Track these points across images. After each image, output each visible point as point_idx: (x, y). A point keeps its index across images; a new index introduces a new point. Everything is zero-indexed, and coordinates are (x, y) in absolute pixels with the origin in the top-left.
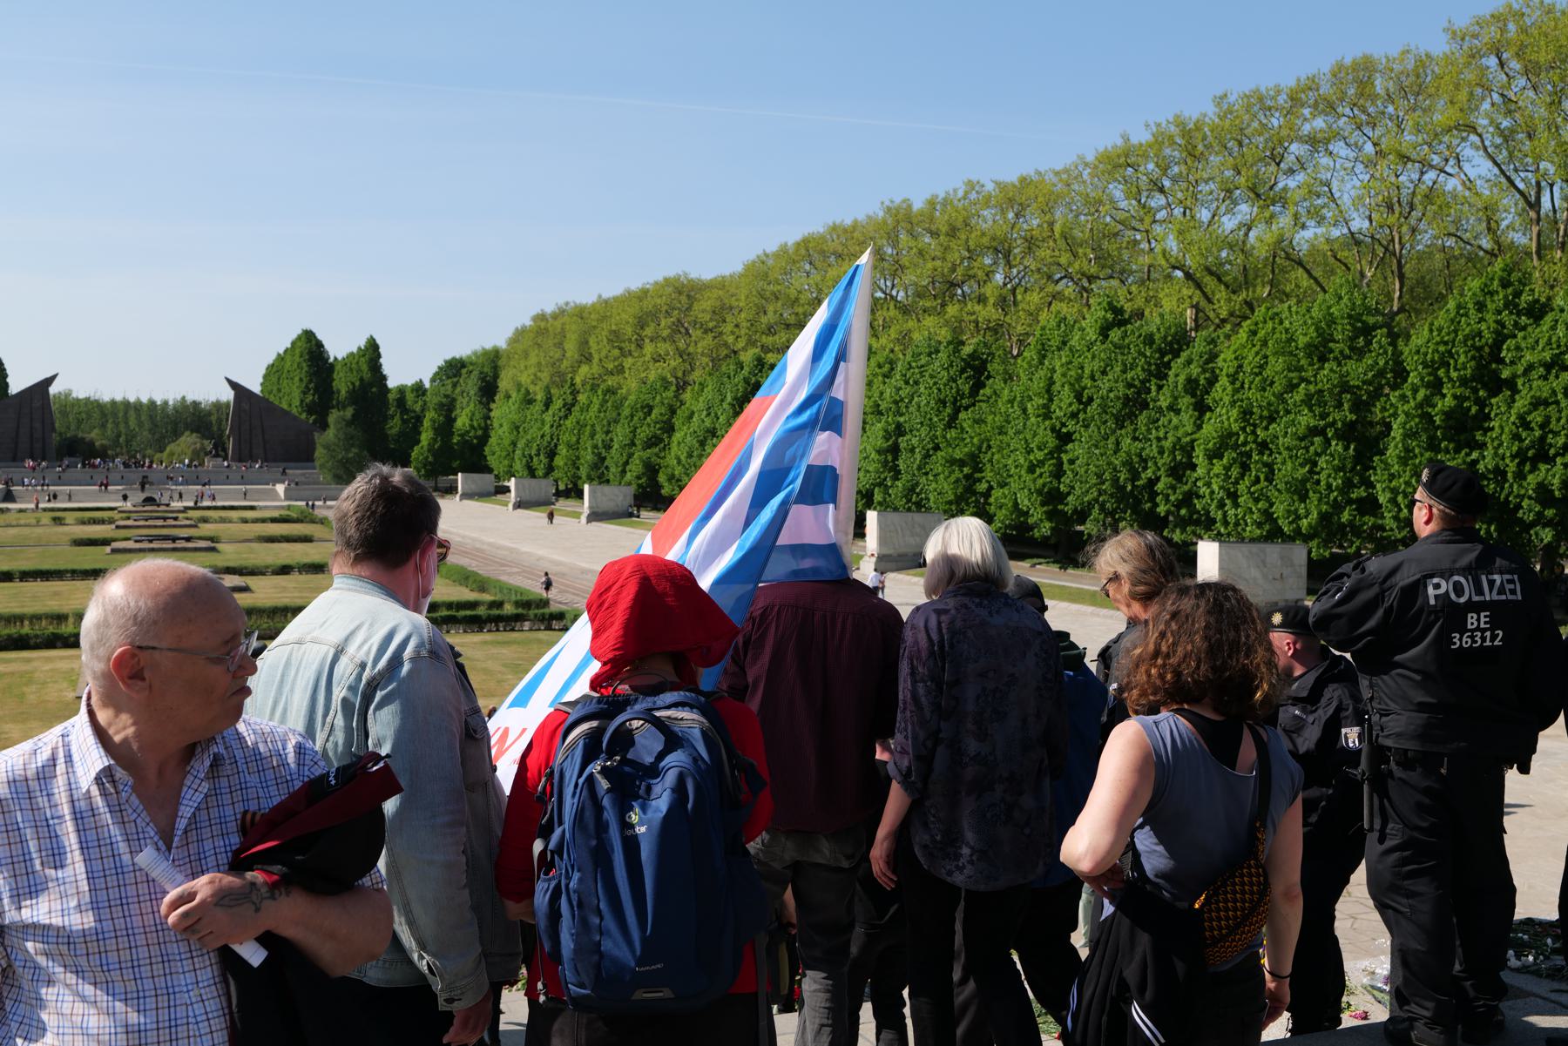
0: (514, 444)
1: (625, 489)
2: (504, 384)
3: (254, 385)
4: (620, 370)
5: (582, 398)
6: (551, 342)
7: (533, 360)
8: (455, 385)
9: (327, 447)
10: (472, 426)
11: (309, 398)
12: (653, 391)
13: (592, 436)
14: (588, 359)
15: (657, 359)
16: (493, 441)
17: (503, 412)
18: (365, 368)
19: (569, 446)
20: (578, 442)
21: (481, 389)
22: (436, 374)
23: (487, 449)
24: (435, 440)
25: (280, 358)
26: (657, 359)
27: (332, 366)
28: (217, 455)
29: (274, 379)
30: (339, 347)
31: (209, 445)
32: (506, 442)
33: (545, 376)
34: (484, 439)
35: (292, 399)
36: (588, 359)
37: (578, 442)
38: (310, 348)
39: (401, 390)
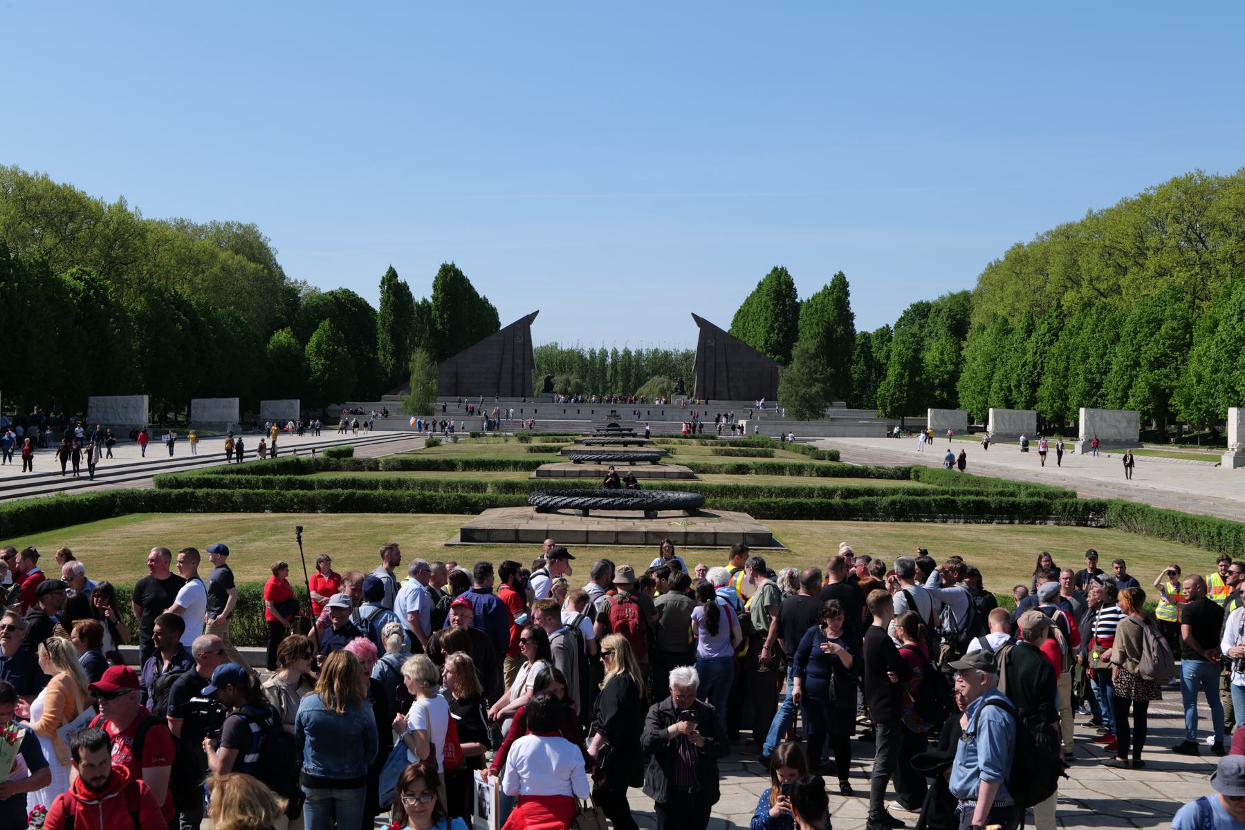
0: (989, 378)
1: (1128, 414)
2: (976, 320)
3: (724, 323)
4: (1117, 290)
5: (1071, 322)
6: (1031, 269)
7: (1010, 290)
8: (921, 327)
9: (790, 381)
10: (942, 361)
11: (774, 337)
12: (1160, 302)
13: (1086, 356)
14: (1077, 283)
15: (1162, 273)
16: (965, 375)
17: (976, 346)
18: (831, 308)
19: (1055, 372)
20: (1067, 369)
21: (950, 328)
22: (901, 319)
23: (959, 385)
24: (901, 375)
25: (748, 302)
26: (1162, 273)
27: (797, 306)
28: (683, 393)
29: (740, 324)
30: (806, 289)
31: (675, 384)
32: (981, 376)
33: (1024, 306)
34: (955, 376)
35: (758, 338)
36: (1077, 283)
37: (1067, 369)
38: (779, 287)
39: (865, 335)
